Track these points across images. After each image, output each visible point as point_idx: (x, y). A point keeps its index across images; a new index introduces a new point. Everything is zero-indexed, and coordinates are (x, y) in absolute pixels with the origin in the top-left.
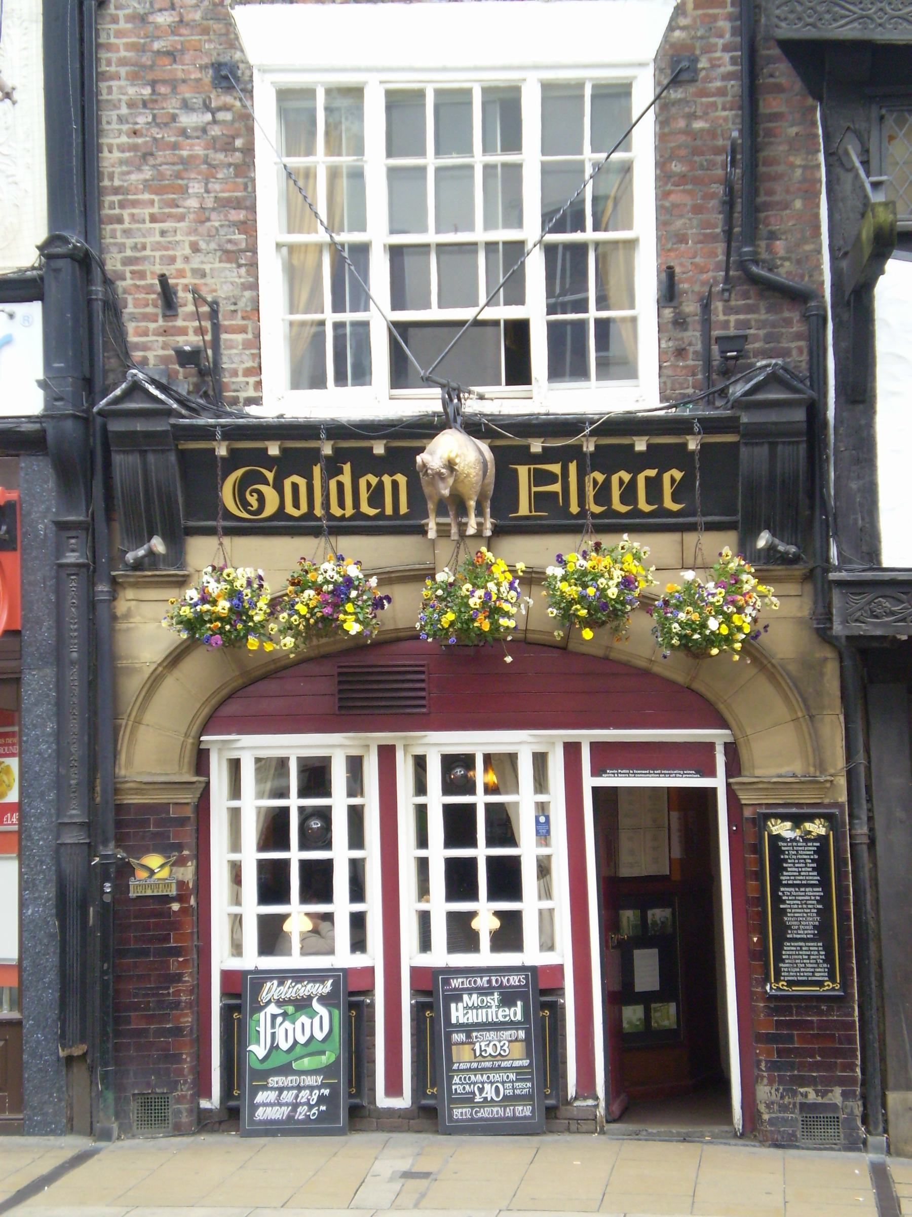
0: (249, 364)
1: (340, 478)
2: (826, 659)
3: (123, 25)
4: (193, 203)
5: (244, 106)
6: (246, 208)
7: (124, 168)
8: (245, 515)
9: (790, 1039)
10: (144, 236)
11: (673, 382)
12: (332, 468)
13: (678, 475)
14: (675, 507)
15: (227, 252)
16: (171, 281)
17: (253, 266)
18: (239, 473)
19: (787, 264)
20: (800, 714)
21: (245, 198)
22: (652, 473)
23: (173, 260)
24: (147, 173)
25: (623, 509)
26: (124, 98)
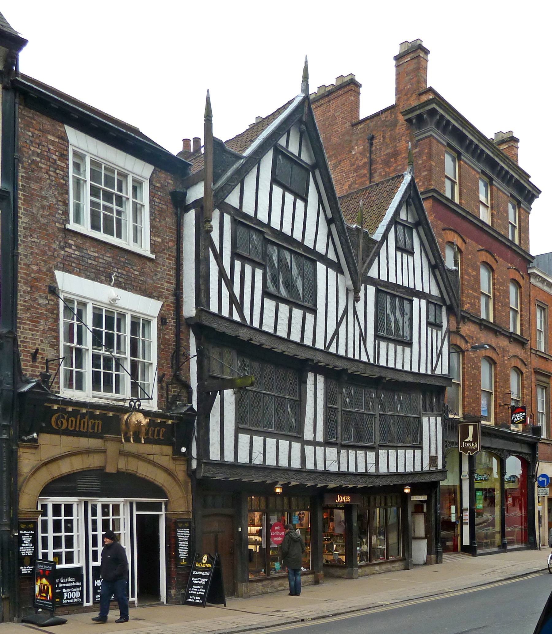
3: (22, 266)
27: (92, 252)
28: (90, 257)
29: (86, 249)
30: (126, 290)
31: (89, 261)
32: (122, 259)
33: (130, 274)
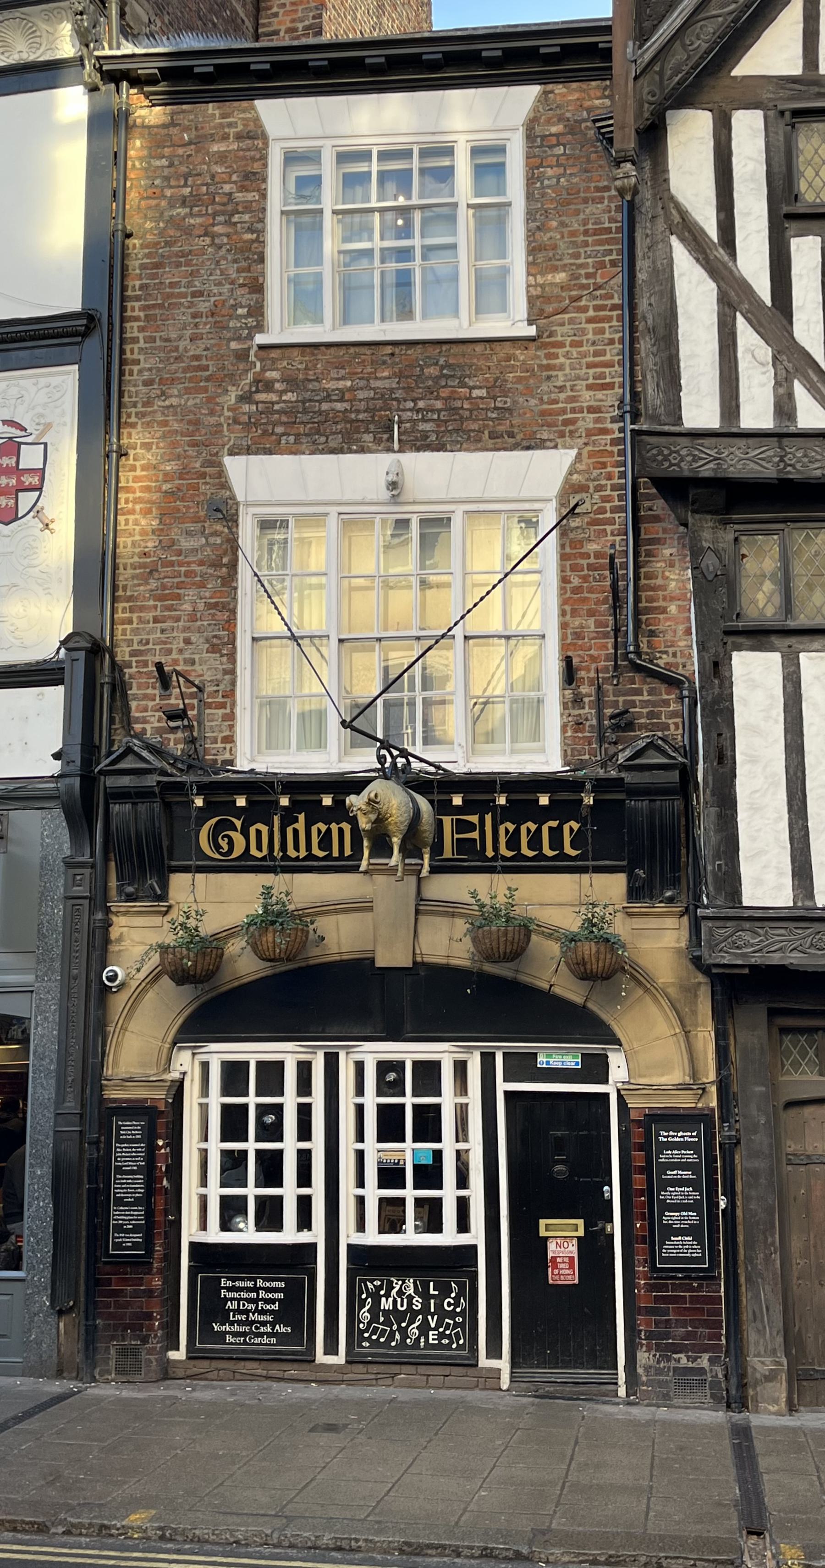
0: (227, 733)
1: (295, 826)
2: (700, 983)
4: (187, 607)
5: (232, 533)
6: (229, 610)
7: (136, 582)
8: (217, 856)
9: (666, 1312)
10: (148, 634)
11: (572, 750)
12: (288, 818)
13: (575, 826)
14: (574, 853)
15: (213, 645)
16: (166, 669)
17: (232, 657)
18: (214, 821)
19: (664, 656)
20: (678, 1031)
21: (229, 603)
22: (554, 824)
23: (169, 652)
24: (153, 584)
25: (531, 854)
26: (137, 528)
27: (338, 379)
28: (329, 396)
29: (317, 380)
30: (446, 451)
31: (325, 406)
32: (433, 371)
33: (458, 404)
